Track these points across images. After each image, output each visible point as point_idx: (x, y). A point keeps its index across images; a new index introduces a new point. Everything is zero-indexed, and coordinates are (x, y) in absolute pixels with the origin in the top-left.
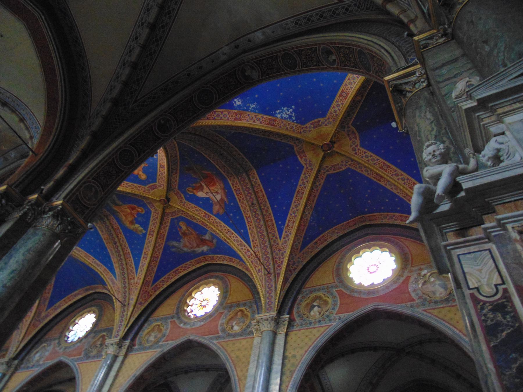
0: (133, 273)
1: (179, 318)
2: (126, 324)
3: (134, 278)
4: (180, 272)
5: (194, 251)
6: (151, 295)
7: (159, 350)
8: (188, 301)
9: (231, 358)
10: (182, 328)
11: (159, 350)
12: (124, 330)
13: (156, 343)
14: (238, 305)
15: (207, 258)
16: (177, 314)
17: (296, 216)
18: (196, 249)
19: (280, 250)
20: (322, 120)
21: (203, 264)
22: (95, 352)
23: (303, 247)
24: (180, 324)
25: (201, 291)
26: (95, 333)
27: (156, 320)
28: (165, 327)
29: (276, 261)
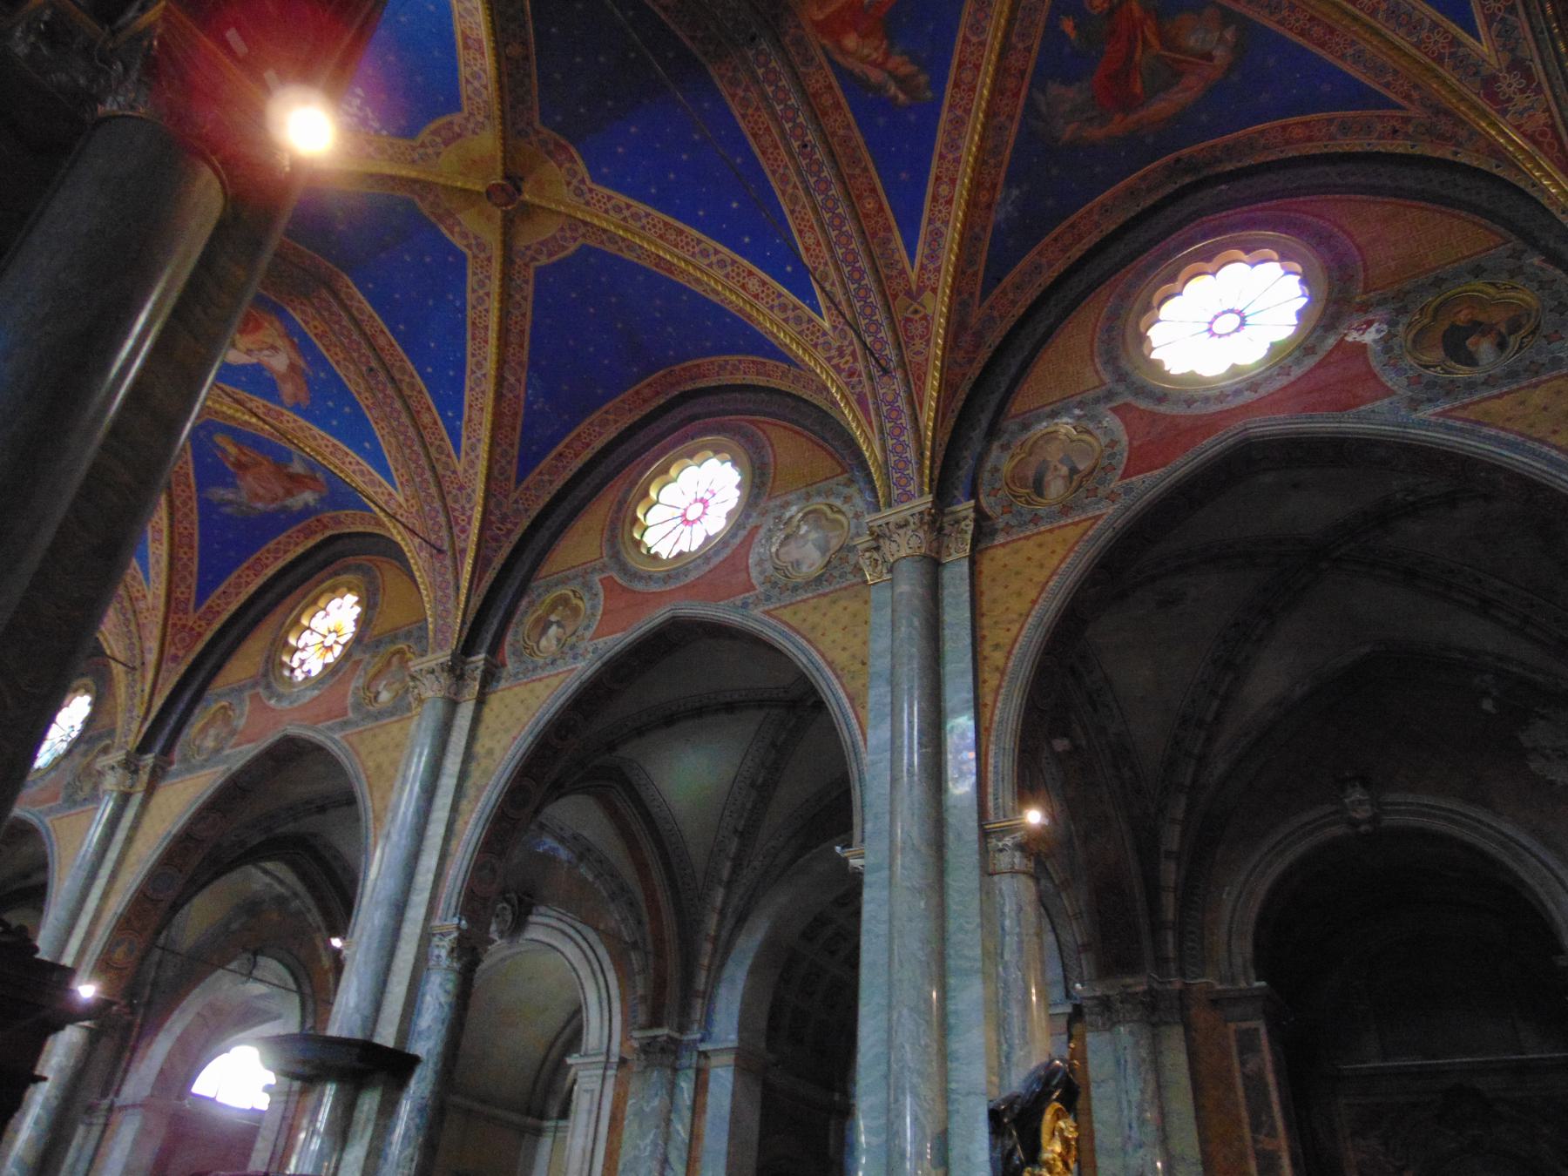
0: (140, 584)
1: (268, 687)
2: (141, 714)
3: (144, 596)
4: (267, 566)
5: (284, 509)
6: (200, 635)
7: (222, 768)
8: (292, 641)
9: (365, 770)
10: (273, 710)
11: (222, 768)
12: (139, 731)
13: (217, 750)
14: (394, 639)
15: (325, 520)
16: (265, 675)
17: (483, 393)
18: (289, 502)
19: (461, 488)
20: (457, 118)
21: (319, 538)
22: (87, 788)
23: (524, 471)
24: (270, 698)
25: (324, 609)
26: (87, 742)
27: (220, 696)
28: (237, 711)
29: (456, 518)
